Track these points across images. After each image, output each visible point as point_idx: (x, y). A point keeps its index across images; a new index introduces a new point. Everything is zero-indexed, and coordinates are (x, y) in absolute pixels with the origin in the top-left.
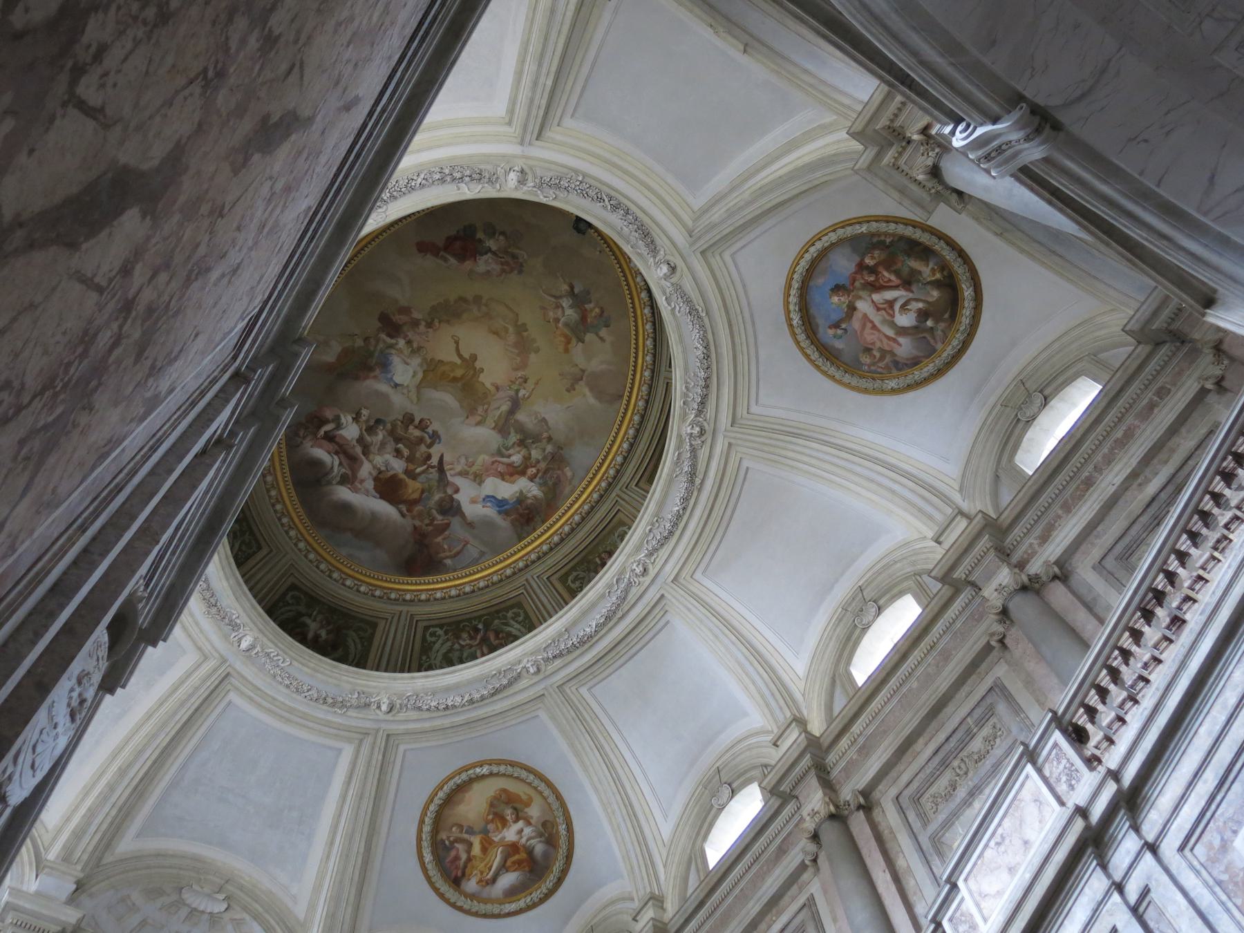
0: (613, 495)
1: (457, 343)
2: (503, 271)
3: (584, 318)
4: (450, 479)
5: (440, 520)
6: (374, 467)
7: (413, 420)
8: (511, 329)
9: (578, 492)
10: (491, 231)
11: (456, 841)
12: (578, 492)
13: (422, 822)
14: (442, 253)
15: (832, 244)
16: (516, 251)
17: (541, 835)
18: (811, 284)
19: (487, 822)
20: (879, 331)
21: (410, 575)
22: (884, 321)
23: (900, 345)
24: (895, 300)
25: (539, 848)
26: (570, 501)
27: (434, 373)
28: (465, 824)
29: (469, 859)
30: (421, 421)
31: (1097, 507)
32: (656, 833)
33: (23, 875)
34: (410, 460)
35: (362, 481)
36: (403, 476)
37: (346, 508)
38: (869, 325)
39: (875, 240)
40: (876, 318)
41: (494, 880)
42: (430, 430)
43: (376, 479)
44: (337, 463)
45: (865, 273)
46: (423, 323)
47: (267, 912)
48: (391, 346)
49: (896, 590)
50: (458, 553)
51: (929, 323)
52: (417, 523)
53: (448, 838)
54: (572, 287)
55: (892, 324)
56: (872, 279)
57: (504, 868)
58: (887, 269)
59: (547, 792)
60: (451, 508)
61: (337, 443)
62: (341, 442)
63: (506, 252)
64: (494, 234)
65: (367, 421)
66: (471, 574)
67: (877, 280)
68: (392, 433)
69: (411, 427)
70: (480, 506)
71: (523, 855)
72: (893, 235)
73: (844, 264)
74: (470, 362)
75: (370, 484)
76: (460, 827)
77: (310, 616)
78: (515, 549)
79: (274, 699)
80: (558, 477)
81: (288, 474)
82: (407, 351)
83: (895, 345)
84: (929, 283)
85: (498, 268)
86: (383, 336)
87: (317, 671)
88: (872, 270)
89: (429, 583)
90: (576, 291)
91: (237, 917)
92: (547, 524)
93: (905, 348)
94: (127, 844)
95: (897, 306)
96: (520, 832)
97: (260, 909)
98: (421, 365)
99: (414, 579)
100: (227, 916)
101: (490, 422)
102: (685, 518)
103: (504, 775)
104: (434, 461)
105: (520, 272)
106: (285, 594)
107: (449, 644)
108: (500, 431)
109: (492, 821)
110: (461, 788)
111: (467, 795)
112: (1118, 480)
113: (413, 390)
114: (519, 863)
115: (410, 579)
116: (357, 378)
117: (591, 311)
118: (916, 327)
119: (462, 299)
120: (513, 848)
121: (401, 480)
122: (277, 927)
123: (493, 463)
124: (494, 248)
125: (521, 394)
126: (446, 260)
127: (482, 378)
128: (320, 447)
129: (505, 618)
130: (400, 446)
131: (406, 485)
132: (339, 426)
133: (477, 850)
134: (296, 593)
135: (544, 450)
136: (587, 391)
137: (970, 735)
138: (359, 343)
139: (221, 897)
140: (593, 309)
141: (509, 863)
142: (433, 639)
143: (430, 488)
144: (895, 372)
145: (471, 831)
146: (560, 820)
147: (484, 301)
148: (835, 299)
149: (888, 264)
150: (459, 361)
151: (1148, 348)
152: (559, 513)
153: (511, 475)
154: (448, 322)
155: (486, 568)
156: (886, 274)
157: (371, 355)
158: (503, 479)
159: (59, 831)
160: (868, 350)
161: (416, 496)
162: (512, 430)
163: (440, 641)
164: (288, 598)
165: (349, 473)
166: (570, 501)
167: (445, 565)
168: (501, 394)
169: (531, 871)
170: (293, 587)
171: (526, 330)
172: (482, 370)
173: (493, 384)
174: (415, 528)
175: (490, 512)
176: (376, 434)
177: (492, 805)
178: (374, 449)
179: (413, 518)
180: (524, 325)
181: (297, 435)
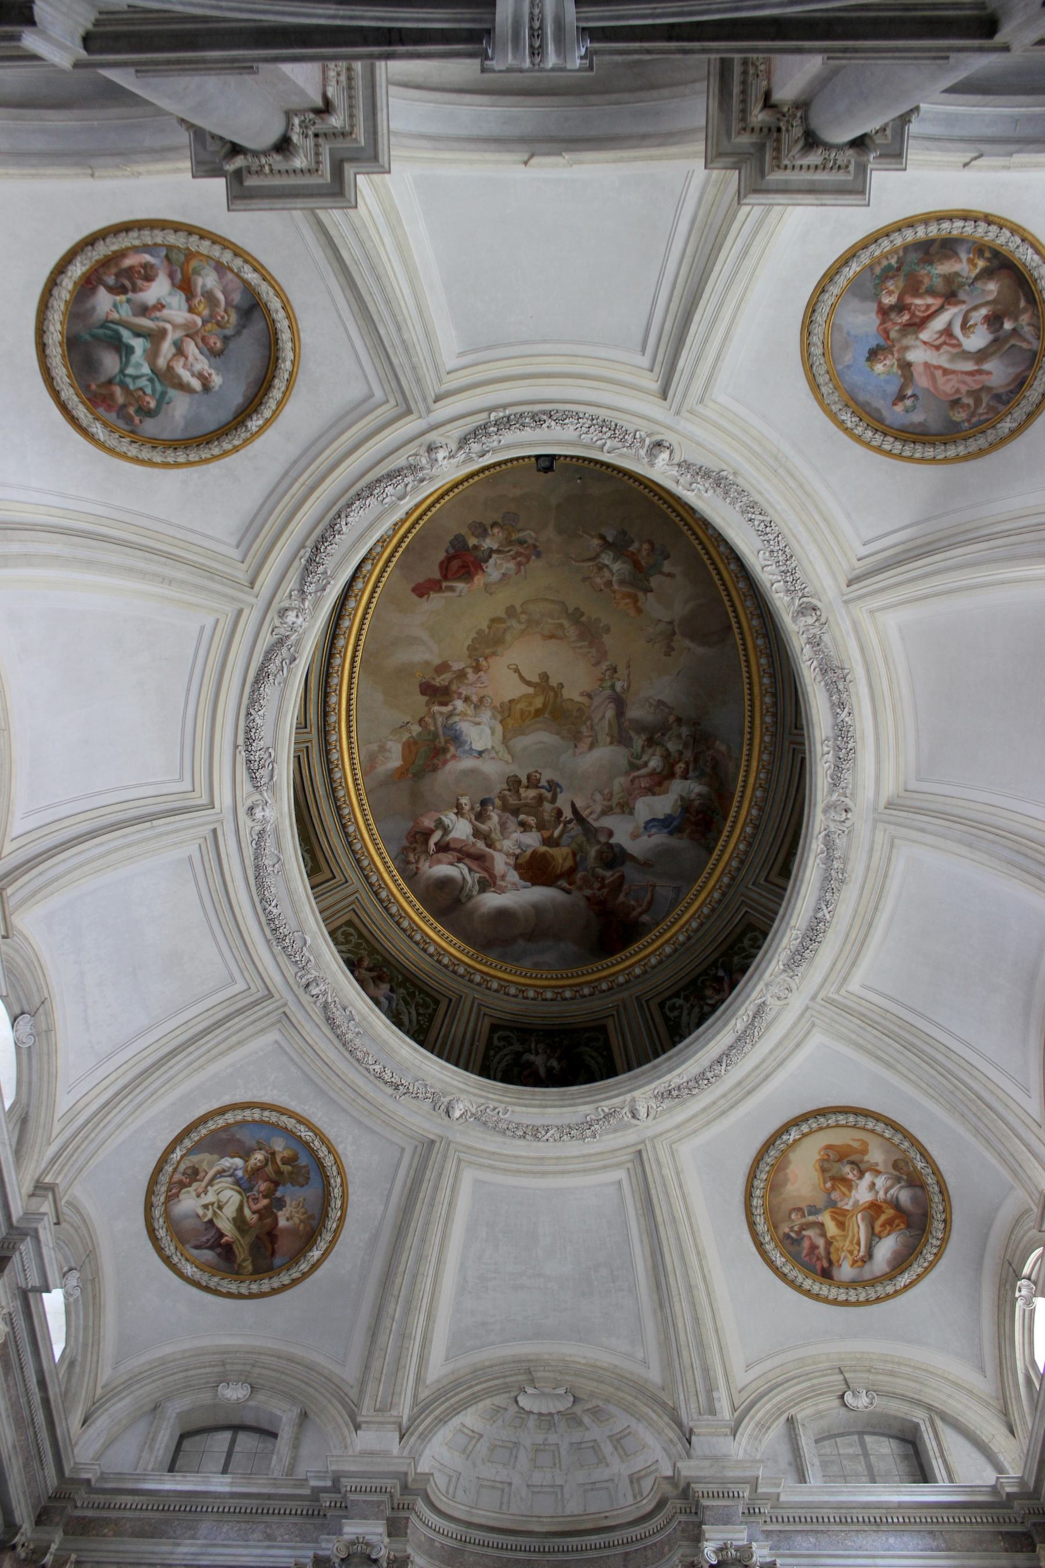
0: (786, 744)
1: (517, 671)
2: (519, 564)
3: (636, 565)
4: (596, 824)
5: (609, 875)
6: (508, 855)
7: (520, 782)
8: (566, 623)
9: (744, 763)
10: (481, 530)
11: (804, 1227)
12: (744, 763)
13: (752, 1225)
14: (444, 584)
16: (521, 535)
17: (898, 1180)
19: (829, 1192)
20: (954, 372)
21: (612, 954)
22: (953, 358)
23: (989, 373)
24: (950, 324)
25: (904, 1196)
26: (741, 778)
27: (512, 718)
28: (803, 1205)
29: (829, 1244)
30: (529, 777)
32: (1024, 1117)
33: (344, 1439)
34: (541, 827)
35: (503, 877)
36: (544, 849)
37: (502, 915)
38: (938, 373)
39: (878, 270)
40: (941, 359)
41: (870, 1255)
42: (543, 783)
43: (517, 867)
44: (466, 871)
45: (893, 315)
46: (469, 670)
47: (618, 1389)
48: (451, 714)
50: (650, 903)
51: (1008, 325)
52: (588, 892)
53: (791, 1229)
54: (602, 537)
55: (965, 355)
56: (906, 317)
57: (874, 1237)
58: (916, 294)
59: (880, 1127)
60: (615, 857)
61: (455, 850)
62: (458, 846)
63: (510, 543)
64: (485, 530)
65: (472, 809)
66: (677, 920)
67: (913, 315)
68: (505, 808)
69: (522, 790)
70: (645, 838)
71: (890, 1212)
72: (894, 251)
73: (862, 321)
74: (543, 684)
75: (513, 876)
76: (799, 1210)
77: (530, 1051)
78: (710, 865)
79: (516, 1157)
80: (713, 758)
81: (422, 909)
82: (470, 711)
83: (984, 377)
84: (977, 278)
85: (512, 565)
86: (436, 708)
87: (546, 1107)
88: (900, 307)
89: (636, 953)
90: (610, 539)
91: (589, 1406)
92: (731, 819)
93: (998, 373)
94: (437, 1369)
95: (957, 331)
96: (873, 1185)
97: (612, 1390)
98: (494, 717)
99: (617, 957)
100: (578, 1409)
101: (603, 737)
102: (857, 724)
103: (821, 1129)
104: (568, 814)
105: (538, 555)
106: (490, 1039)
107: (696, 1010)
108: (620, 742)
109: (833, 1188)
110: (780, 1166)
111: (788, 1171)
113: (500, 748)
114: (889, 1222)
115: (613, 959)
116: (435, 769)
117: (639, 550)
118: (995, 340)
119: (493, 621)
120: (874, 1208)
121: (544, 854)
122: (637, 1402)
123: (632, 781)
124: (495, 547)
125: (618, 689)
126: (452, 589)
127: (566, 694)
128: (439, 862)
129: (743, 949)
130: (522, 817)
131: (552, 856)
132: (446, 831)
133: (832, 1229)
134: (500, 1033)
135: (679, 736)
136: (687, 643)
138: (416, 729)
139: (561, 1391)
140: (640, 548)
141: (877, 1229)
142: (676, 1013)
143: (581, 847)
144: (1001, 407)
145: (814, 1210)
146: (913, 1153)
147: (519, 609)
148: (879, 368)
149: (914, 287)
150: (531, 690)
152: (737, 798)
153: (660, 784)
154: (494, 654)
155: (690, 905)
156: (918, 301)
157: (436, 735)
158: (654, 794)
159: (363, 1383)
161: (569, 863)
162: (632, 733)
163: (685, 1012)
164: (496, 1042)
165: (485, 875)
166: (741, 778)
167: (644, 924)
168: (597, 701)
169: (908, 1226)
170: (494, 1028)
171: (582, 614)
172: (561, 686)
173: (582, 694)
174: (588, 898)
175: (659, 838)
176: (489, 818)
177: (823, 1170)
178: (496, 835)
179: (580, 889)
180: (577, 609)
181: (408, 863)
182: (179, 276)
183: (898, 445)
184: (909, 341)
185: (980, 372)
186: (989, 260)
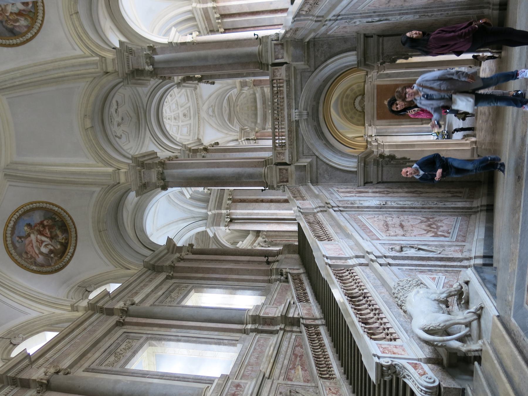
15: (42, 207)
18: (23, 217)
31: (144, 296)
38: (31, 245)
39: (53, 216)
40: (35, 244)
45: (41, 226)
49: (104, 283)
51: (52, 255)
55: (39, 249)
56: (42, 229)
58: (49, 230)
73: (37, 217)
84: (59, 242)
88: (44, 227)
93: (40, 259)
95: (44, 244)
112: (150, 290)
118: (47, 254)
137: (119, 345)
148: (26, 228)
149: (51, 227)
151: (146, 269)
156: (47, 231)
160: (26, 253)
182: (24, 13)
183: (10, 242)
184: (36, 233)
185: (37, 255)
186: (65, 242)
